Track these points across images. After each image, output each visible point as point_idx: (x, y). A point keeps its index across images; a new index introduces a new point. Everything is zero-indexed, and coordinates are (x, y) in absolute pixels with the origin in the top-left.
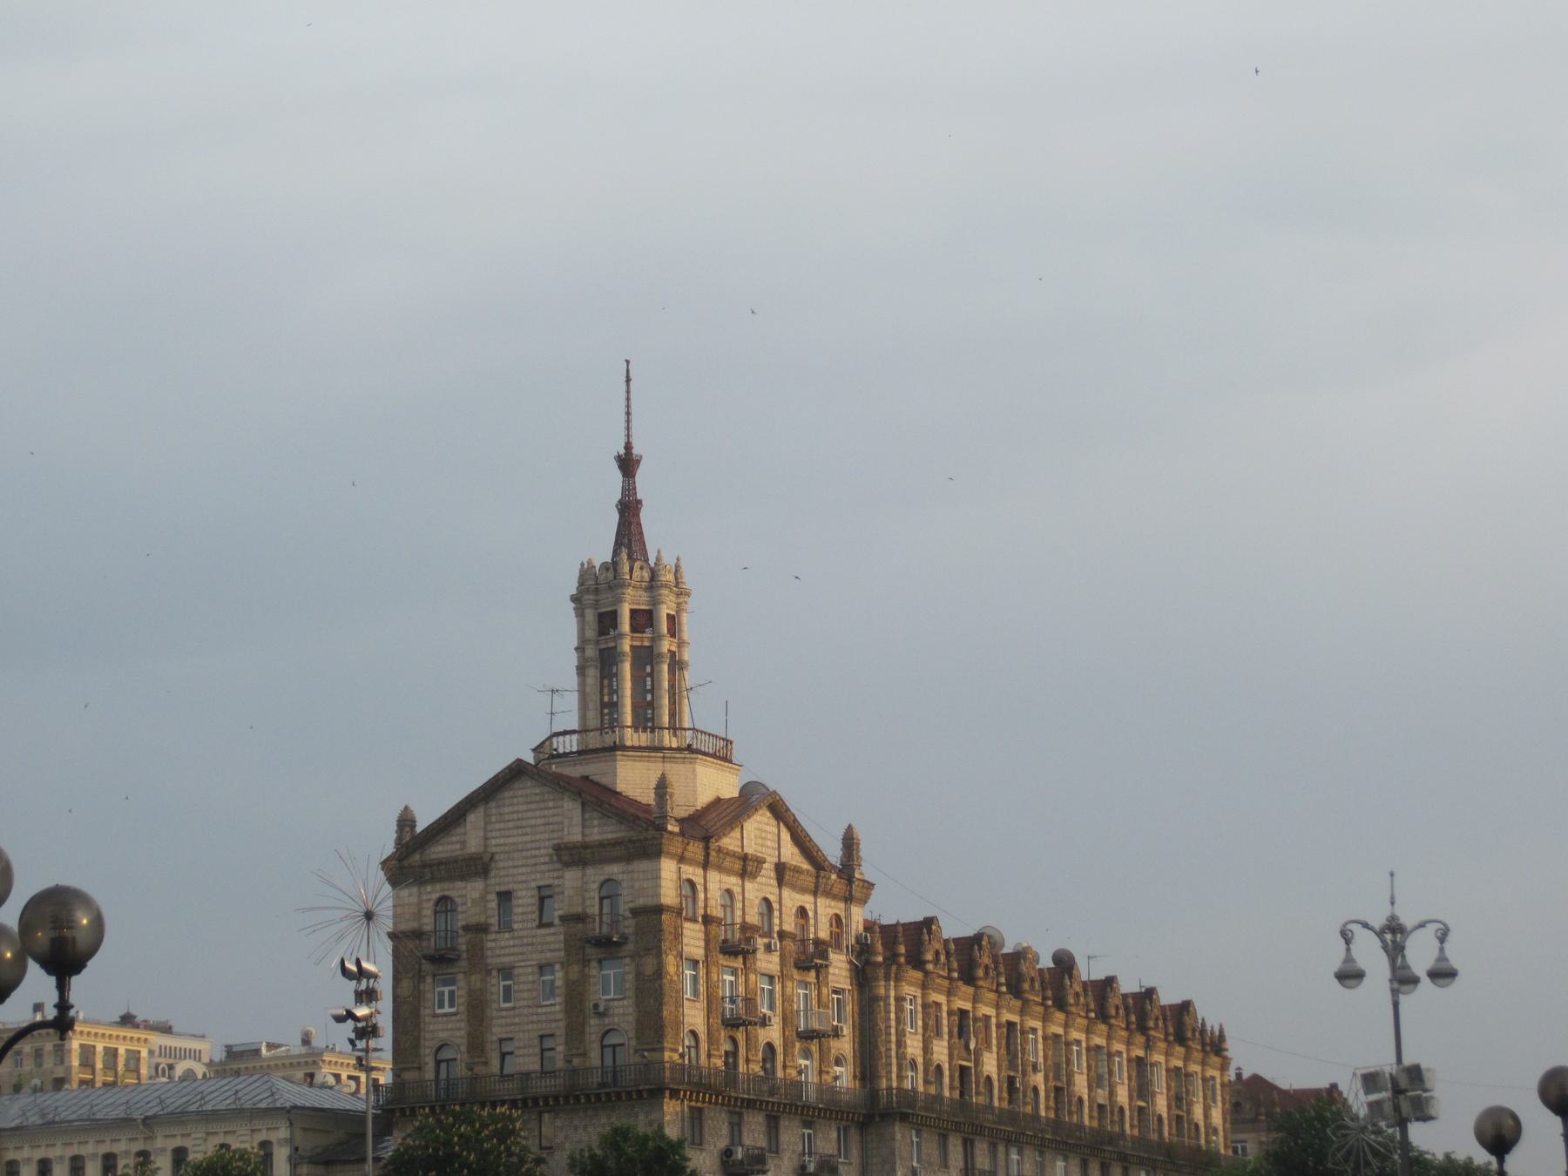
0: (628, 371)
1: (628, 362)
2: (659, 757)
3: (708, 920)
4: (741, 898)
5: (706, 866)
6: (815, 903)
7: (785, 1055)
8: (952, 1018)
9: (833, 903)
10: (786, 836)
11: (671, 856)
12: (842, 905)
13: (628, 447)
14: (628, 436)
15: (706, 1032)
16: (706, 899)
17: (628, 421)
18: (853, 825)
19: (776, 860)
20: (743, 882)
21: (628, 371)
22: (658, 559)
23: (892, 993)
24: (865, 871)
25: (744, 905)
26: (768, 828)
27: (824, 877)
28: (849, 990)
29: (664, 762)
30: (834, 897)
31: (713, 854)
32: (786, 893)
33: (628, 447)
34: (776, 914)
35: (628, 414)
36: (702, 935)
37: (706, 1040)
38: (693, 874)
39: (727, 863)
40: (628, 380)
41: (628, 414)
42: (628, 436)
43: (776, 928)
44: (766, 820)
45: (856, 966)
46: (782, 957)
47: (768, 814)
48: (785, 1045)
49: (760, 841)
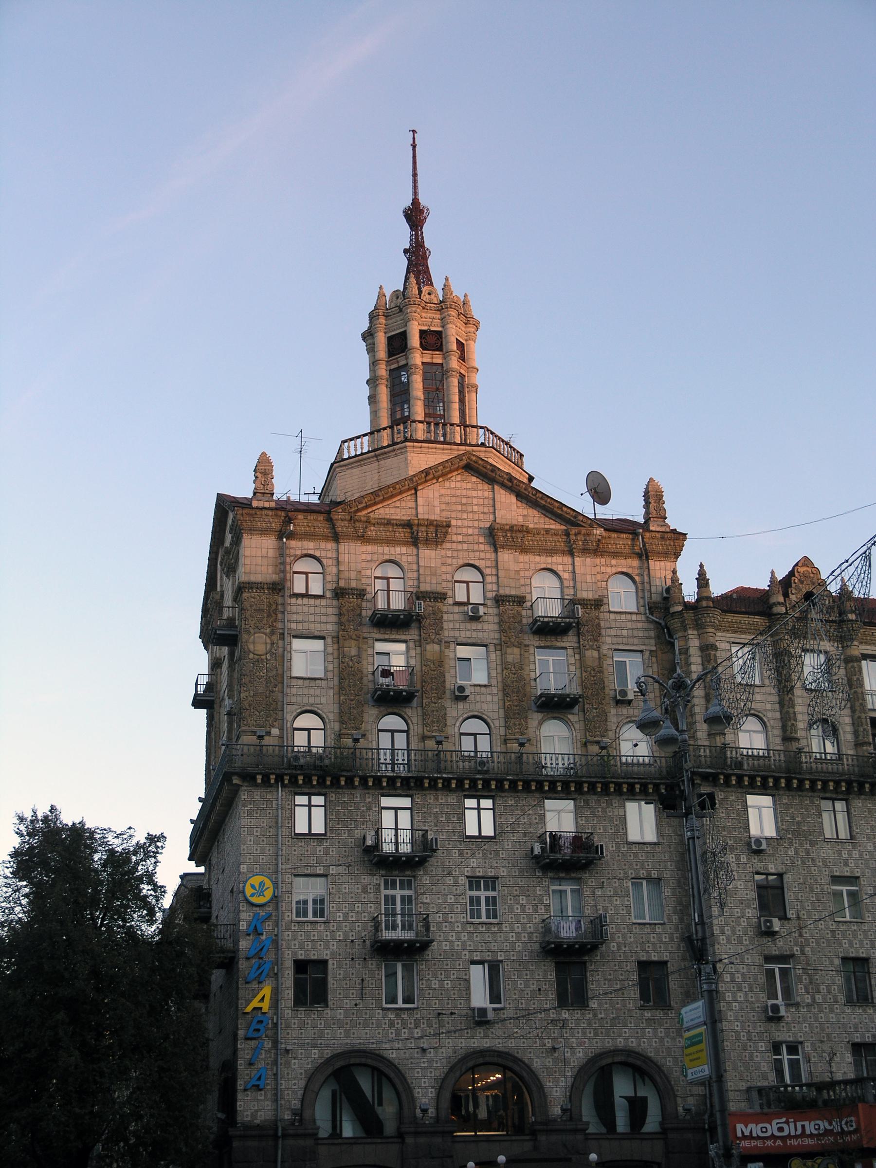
0: (414, 138)
1: (414, 132)
2: (372, 457)
3: (339, 593)
4: (415, 567)
5: (336, 538)
6: (573, 564)
7: (507, 727)
8: (850, 665)
9: (614, 562)
10: (507, 500)
11: (264, 532)
12: (635, 563)
13: (415, 202)
14: (415, 193)
15: (337, 711)
16: (339, 571)
17: (415, 182)
18: (656, 480)
19: (488, 525)
20: (418, 548)
21: (414, 138)
22: (446, 288)
23: (694, 644)
24: (674, 522)
25: (419, 575)
26: (474, 493)
27: (579, 533)
28: (651, 651)
29: (378, 461)
30: (616, 555)
31: (339, 524)
32: (506, 557)
33: (415, 202)
34: (489, 579)
35: (415, 175)
36: (336, 611)
37: (337, 719)
38: (315, 549)
39: (372, 532)
40: (414, 146)
41: (415, 175)
42: (415, 193)
43: (490, 595)
44: (469, 486)
45: (660, 624)
46: (501, 623)
47: (474, 479)
48: (507, 717)
49: (459, 508)
